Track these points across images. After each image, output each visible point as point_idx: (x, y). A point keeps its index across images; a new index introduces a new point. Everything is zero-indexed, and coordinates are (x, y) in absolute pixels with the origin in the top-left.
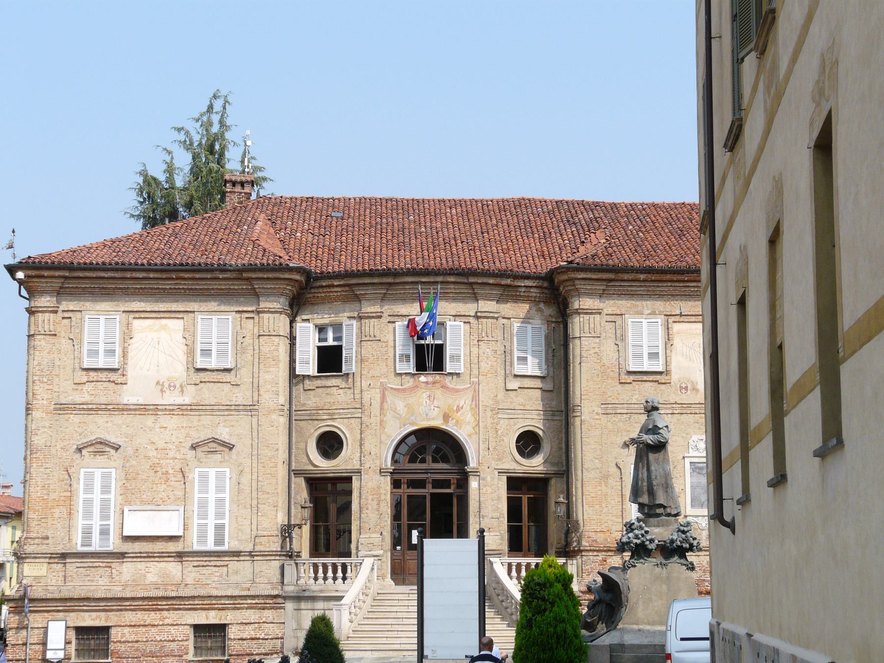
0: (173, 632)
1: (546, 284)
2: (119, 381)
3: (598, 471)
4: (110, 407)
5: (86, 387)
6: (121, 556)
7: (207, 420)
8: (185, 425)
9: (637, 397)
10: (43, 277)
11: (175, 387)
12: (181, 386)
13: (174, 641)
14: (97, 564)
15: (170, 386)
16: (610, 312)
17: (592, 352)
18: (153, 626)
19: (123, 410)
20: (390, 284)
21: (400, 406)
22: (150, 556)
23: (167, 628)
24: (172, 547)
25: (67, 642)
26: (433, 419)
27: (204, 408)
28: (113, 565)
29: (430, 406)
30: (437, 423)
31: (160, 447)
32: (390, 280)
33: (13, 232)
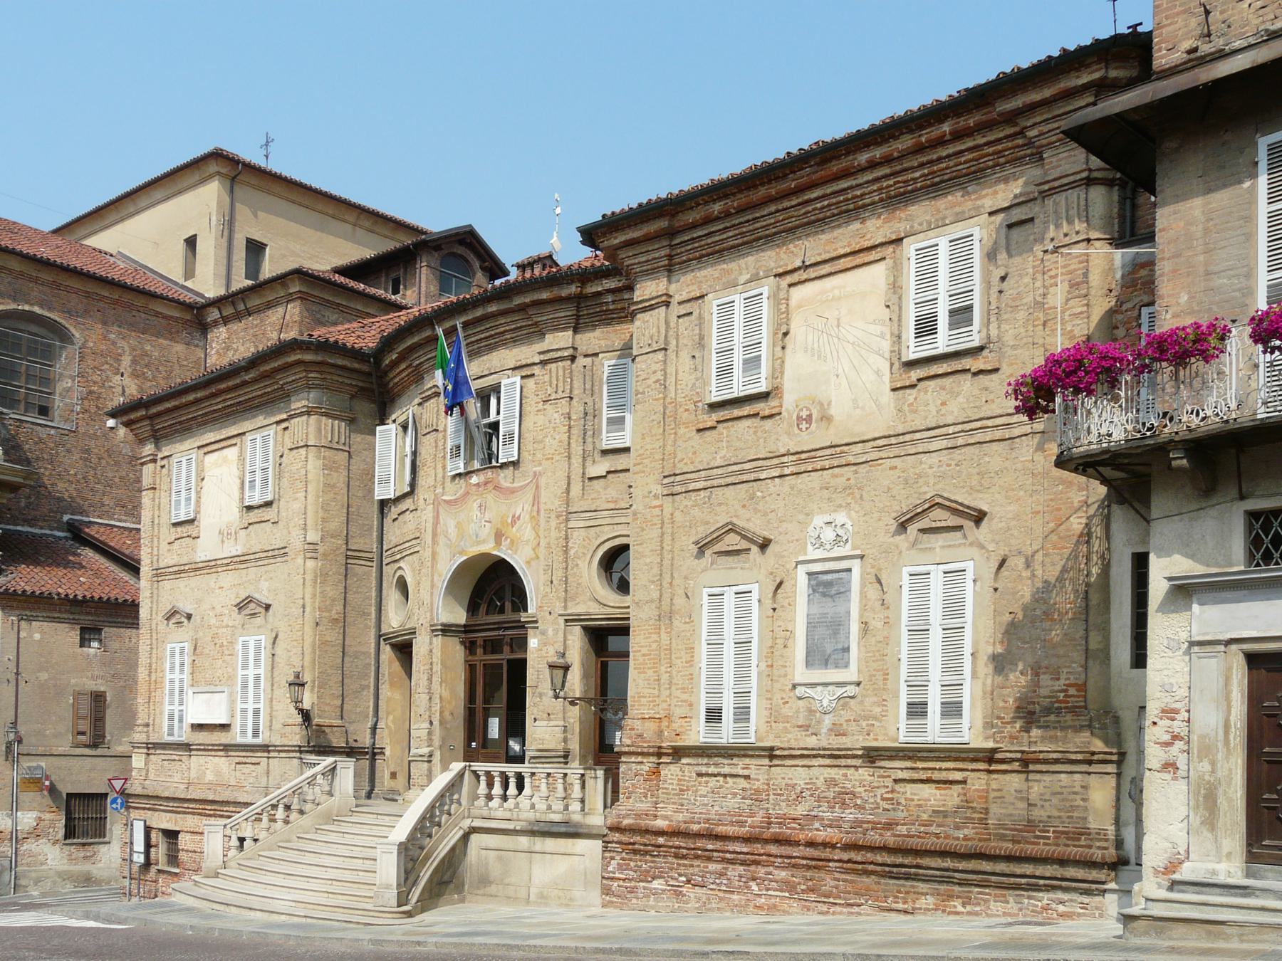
3: (653, 606)
9: (723, 452)
16: (685, 296)
17: (653, 378)
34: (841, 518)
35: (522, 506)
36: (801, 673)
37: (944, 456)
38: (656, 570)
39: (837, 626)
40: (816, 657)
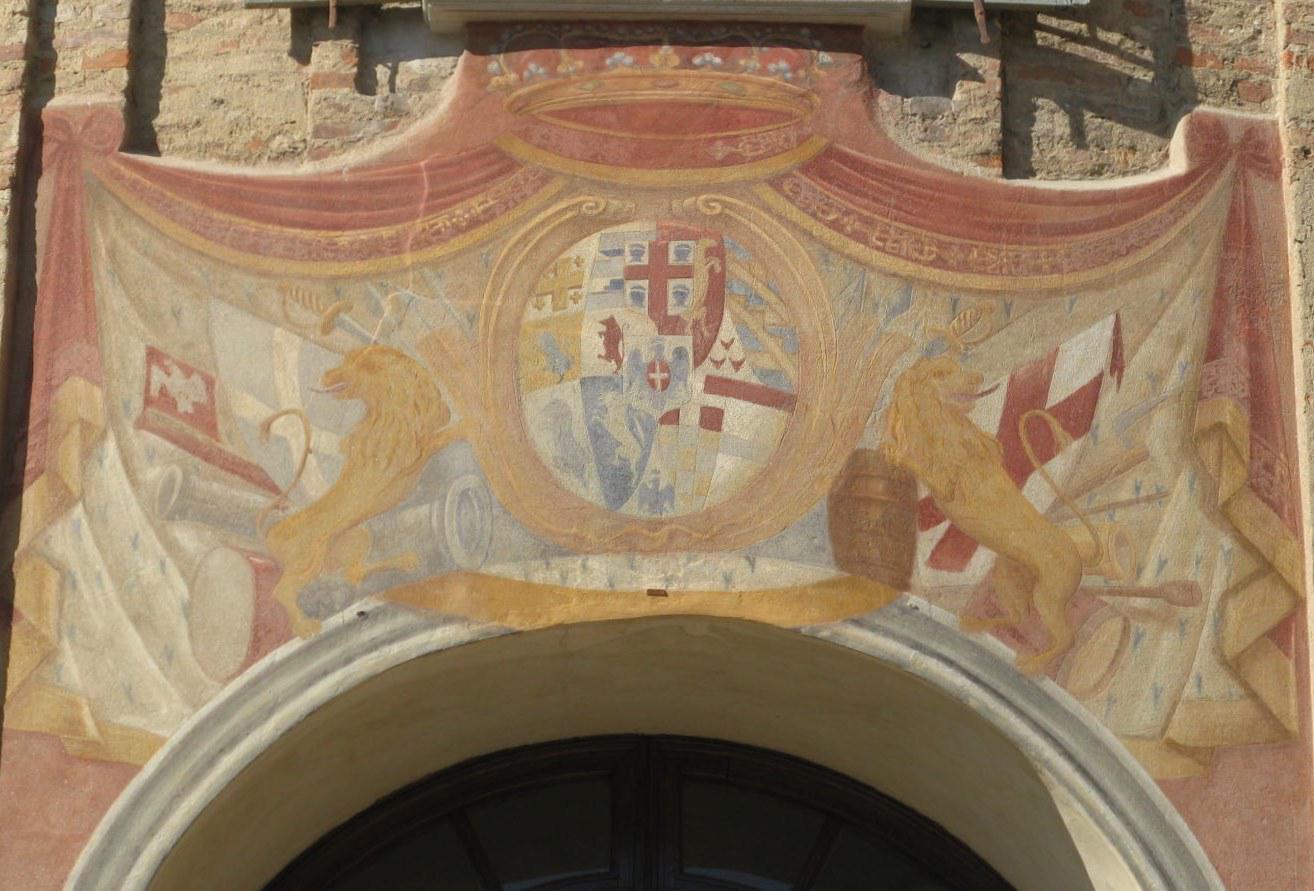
26: (710, 533)
29: (661, 376)
30: (769, 579)
35: (1114, 340)
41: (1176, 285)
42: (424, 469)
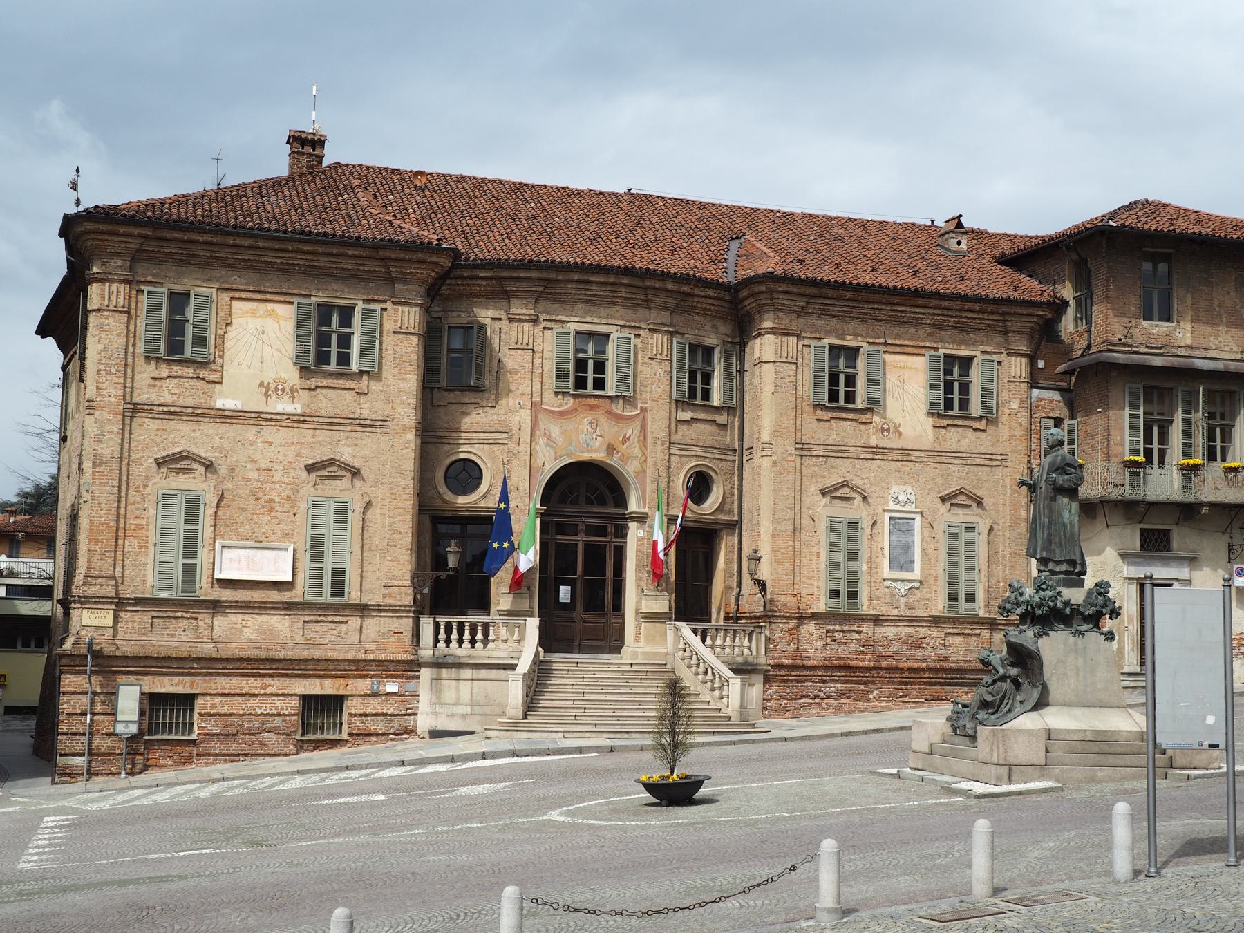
0: (278, 703)
1: (727, 297)
2: (212, 378)
4: (199, 411)
5: (166, 384)
6: (215, 607)
7: (323, 435)
8: (295, 440)
10: (117, 234)
11: (283, 390)
12: (291, 390)
13: (279, 715)
14: (179, 614)
15: (277, 389)
18: (254, 695)
19: (216, 416)
20: (549, 280)
21: (556, 431)
22: (248, 606)
23: (270, 699)
24: (275, 596)
25: (141, 714)
26: (596, 451)
27: (321, 420)
28: (200, 616)
30: (599, 456)
31: (264, 466)
32: (552, 275)
33: (78, 171)
34: (909, 490)
35: (632, 430)
36: (886, 573)
37: (960, 467)
38: (791, 501)
39: (907, 548)
40: (895, 564)
41: (638, 424)
42: (571, 444)
